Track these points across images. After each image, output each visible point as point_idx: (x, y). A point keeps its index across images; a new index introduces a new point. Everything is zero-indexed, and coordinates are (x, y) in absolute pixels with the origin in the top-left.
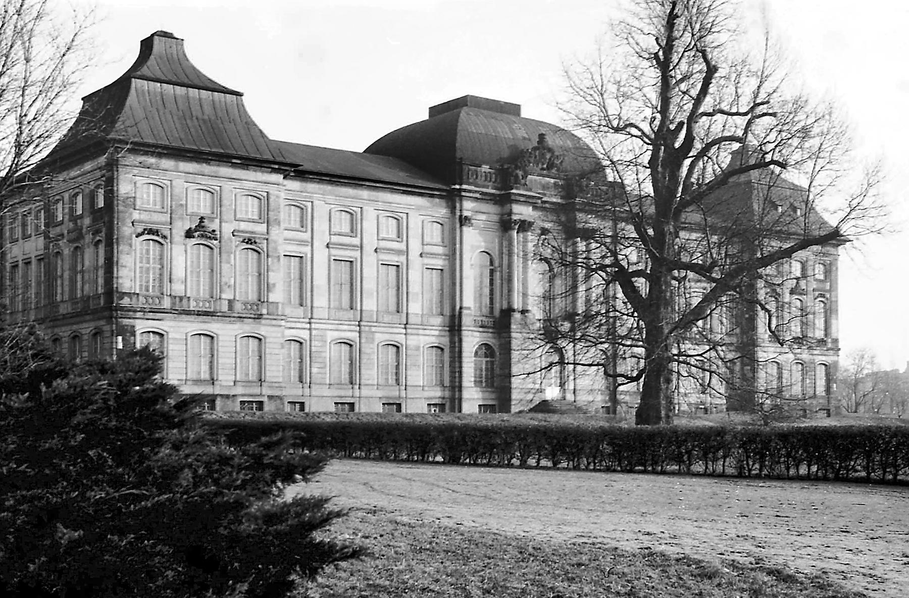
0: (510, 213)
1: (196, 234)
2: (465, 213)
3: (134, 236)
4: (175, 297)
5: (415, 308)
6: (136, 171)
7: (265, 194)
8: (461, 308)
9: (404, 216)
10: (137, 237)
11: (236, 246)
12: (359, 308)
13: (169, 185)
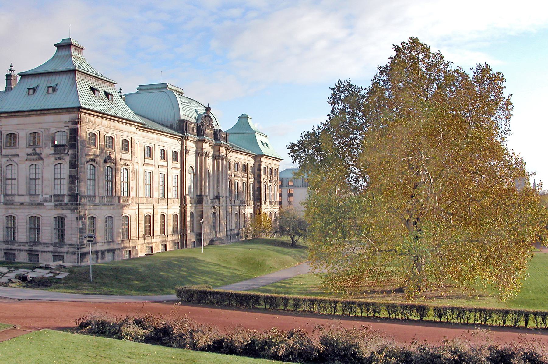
0: (202, 149)
3: (86, 163)
5: (170, 195)
6: (87, 126)
8: (186, 195)
10: (87, 163)
11: (121, 167)
12: (153, 197)
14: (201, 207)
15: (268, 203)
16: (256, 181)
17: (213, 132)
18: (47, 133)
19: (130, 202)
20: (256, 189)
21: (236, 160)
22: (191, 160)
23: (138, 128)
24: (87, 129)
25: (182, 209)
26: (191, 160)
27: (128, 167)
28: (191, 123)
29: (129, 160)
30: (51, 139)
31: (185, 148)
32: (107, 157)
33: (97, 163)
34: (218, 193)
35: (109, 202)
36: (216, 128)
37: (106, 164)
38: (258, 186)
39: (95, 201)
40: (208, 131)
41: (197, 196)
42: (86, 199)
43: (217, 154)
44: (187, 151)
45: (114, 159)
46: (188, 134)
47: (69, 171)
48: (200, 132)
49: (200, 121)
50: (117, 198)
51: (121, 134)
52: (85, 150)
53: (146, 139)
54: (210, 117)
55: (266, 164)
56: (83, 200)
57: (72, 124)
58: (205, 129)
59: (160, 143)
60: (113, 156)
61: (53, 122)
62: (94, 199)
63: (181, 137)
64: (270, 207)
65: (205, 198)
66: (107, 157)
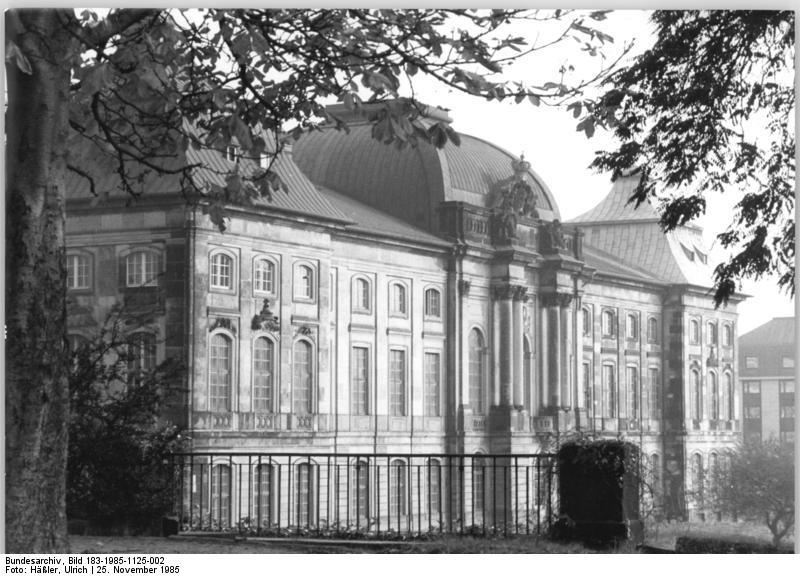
0: (507, 277)
1: (263, 324)
2: (466, 278)
3: (208, 330)
4: (243, 414)
6: (210, 238)
7: (316, 263)
9: (409, 282)
10: (210, 331)
12: (374, 413)
13: (238, 254)
14: (504, 440)
15: (705, 425)
16: (667, 362)
17: (536, 231)
18: (108, 257)
19: (316, 428)
20: (667, 380)
21: (606, 302)
22: (473, 312)
23: (335, 235)
24: (211, 247)
25: (452, 446)
26: (473, 312)
27: (311, 338)
28: (474, 209)
29: (314, 320)
30: (117, 271)
31: (458, 278)
32: (258, 313)
33: (234, 330)
34: (553, 398)
35: (263, 427)
36: (546, 216)
37: (259, 331)
38: (672, 377)
39: (229, 425)
40: (523, 228)
41: (493, 407)
42: (207, 420)
43: (549, 289)
44: (464, 287)
45: (276, 318)
46: (467, 242)
47: (166, 350)
48: (499, 230)
49: (500, 202)
50: (284, 418)
51: (293, 251)
52: (205, 299)
53: (353, 261)
54: (528, 189)
55: (694, 311)
56: (200, 423)
57: (173, 237)
58: (513, 223)
59: (393, 271)
60: (274, 311)
61: (122, 231)
62: (226, 421)
63: (448, 249)
64: (713, 439)
65: (514, 414)
66: (258, 313)
